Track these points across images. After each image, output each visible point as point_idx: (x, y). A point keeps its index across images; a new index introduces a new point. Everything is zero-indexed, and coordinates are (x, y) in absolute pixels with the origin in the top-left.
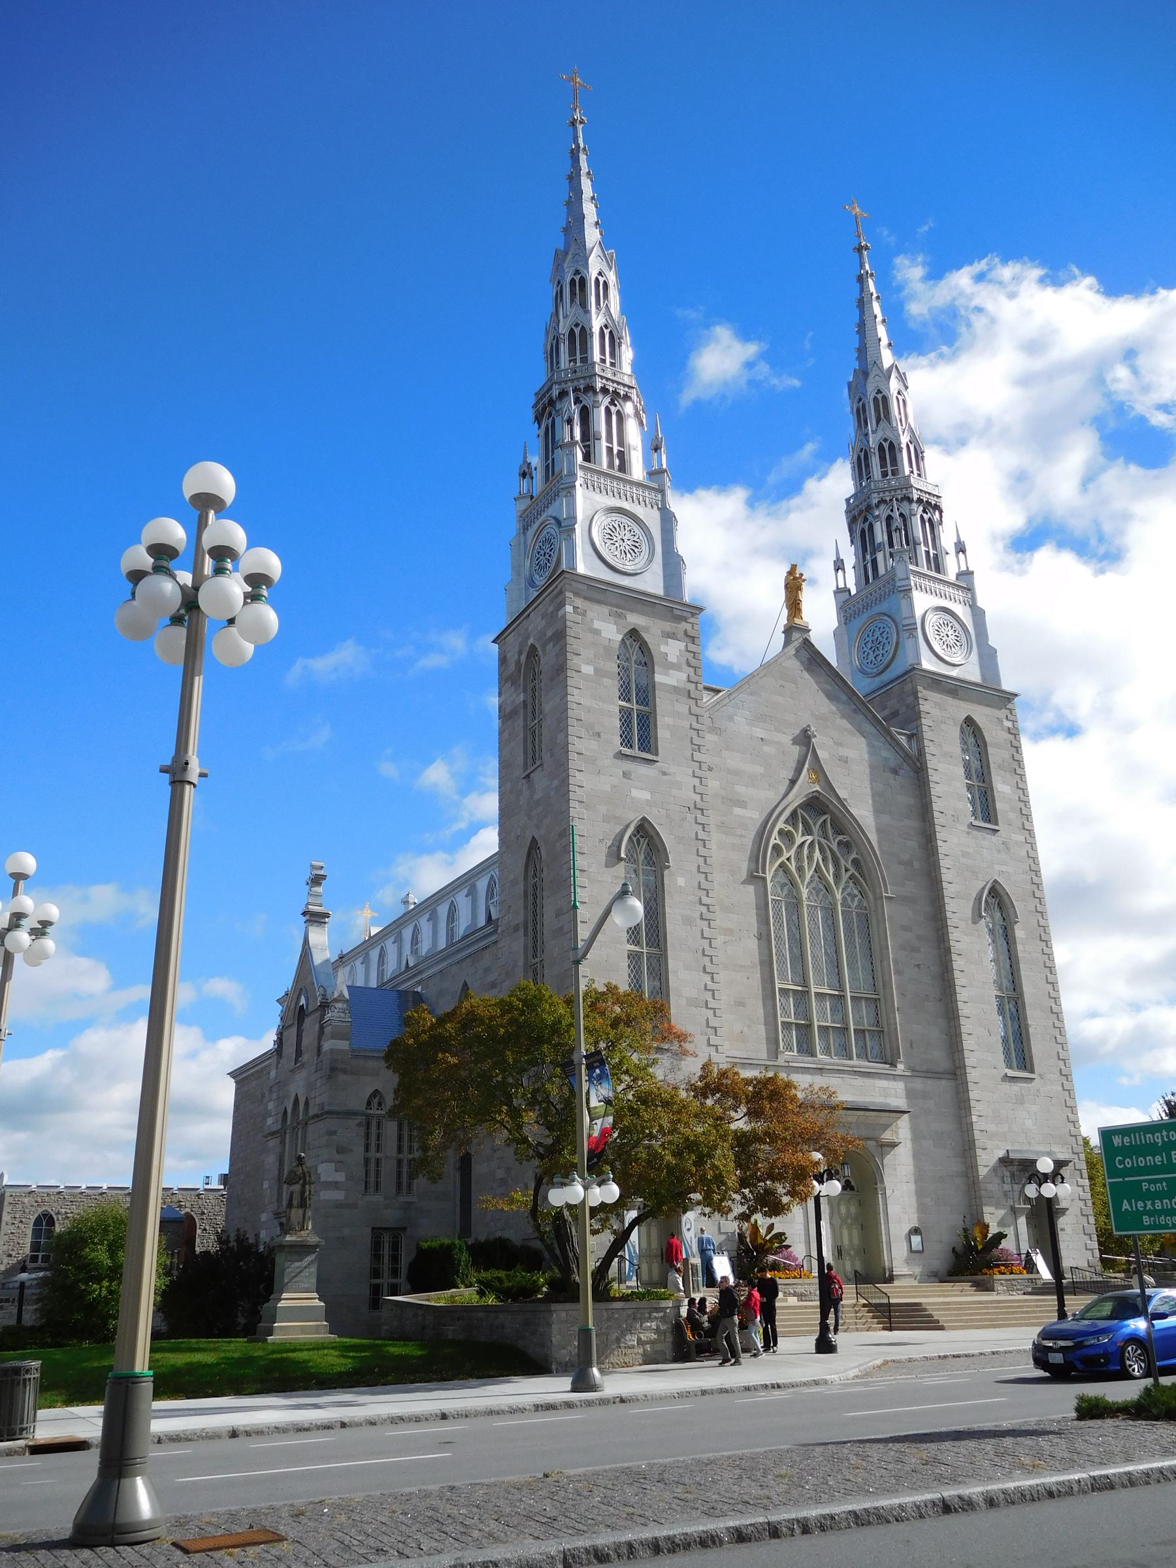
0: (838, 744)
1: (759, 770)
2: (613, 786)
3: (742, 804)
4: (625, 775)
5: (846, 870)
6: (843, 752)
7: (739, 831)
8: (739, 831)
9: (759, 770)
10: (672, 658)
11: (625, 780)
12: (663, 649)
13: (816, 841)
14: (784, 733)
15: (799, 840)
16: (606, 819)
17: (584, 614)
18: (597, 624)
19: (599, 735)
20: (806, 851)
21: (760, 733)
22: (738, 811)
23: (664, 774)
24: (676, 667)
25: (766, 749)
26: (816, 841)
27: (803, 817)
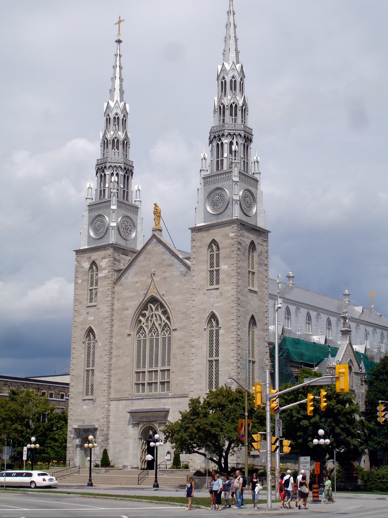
0: (164, 272)
1: (134, 294)
2: (84, 318)
3: (127, 309)
4: (88, 313)
5: (164, 321)
6: (165, 275)
7: (125, 319)
8: (125, 319)
9: (134, 294)
10: (104, 267)
11: (87, 315)
12: (101, 264)
13: (154, 314)
14: (144, 276)
15: (147, 316)
16: (81, 330)
17: (80, 263)
18: (84, 264)
19: (81, 303)
20: (150, 318)
21: (136, 279)
22: (126, 312)
23: (98, 309)
24: (105, 269)
25: (138, 285)
26: (154, 314)
27: (150, 306)
